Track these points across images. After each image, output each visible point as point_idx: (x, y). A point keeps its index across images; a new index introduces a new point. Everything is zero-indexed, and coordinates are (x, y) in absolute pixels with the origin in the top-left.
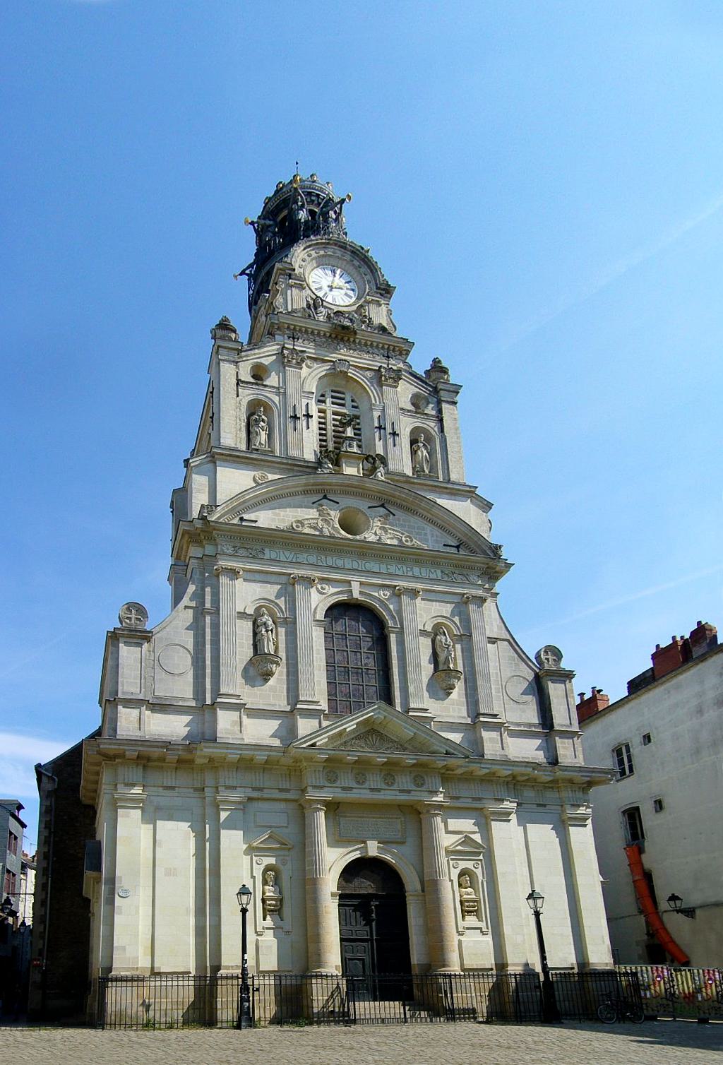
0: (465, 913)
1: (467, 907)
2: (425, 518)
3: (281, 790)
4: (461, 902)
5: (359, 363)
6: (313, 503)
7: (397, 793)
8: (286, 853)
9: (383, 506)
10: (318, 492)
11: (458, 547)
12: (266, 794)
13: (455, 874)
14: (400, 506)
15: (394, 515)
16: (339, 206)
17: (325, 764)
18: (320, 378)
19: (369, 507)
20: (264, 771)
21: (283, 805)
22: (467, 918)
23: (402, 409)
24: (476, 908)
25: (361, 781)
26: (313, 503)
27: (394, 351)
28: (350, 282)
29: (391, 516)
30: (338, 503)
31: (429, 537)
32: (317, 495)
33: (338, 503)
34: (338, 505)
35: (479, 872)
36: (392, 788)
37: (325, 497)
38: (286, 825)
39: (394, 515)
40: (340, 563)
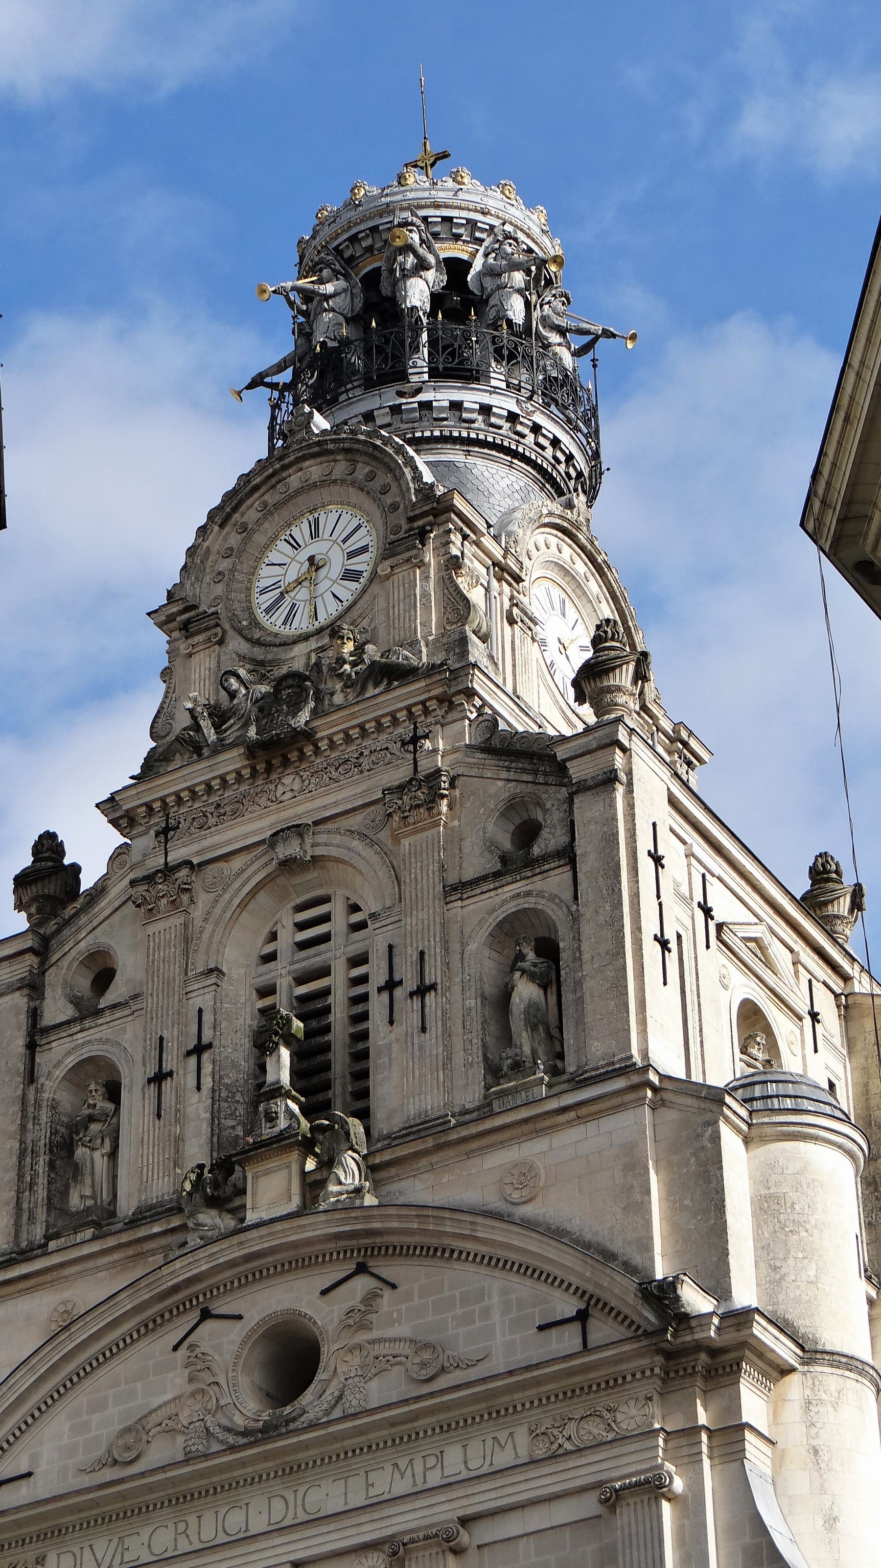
2: (479, 1259)
5: (336, 804)
6: (175, 1348)
9: (362, 1269)
10: (180, 1309)
11: (582, 1317)
14: (404, 1252)
15: (394, 1286)
18: (243, 905)
19: (324, 1293)
23: (454, 888)
26: (175, 1348)
29: (387, 1293)
30: (239, 1317)
31: (496, 1317)
32: (178, 1322)
33: (239, 1317)
34: (237, 1325)
37: (206, 1315)
39: (394, 1286)
40: (235, 1521)
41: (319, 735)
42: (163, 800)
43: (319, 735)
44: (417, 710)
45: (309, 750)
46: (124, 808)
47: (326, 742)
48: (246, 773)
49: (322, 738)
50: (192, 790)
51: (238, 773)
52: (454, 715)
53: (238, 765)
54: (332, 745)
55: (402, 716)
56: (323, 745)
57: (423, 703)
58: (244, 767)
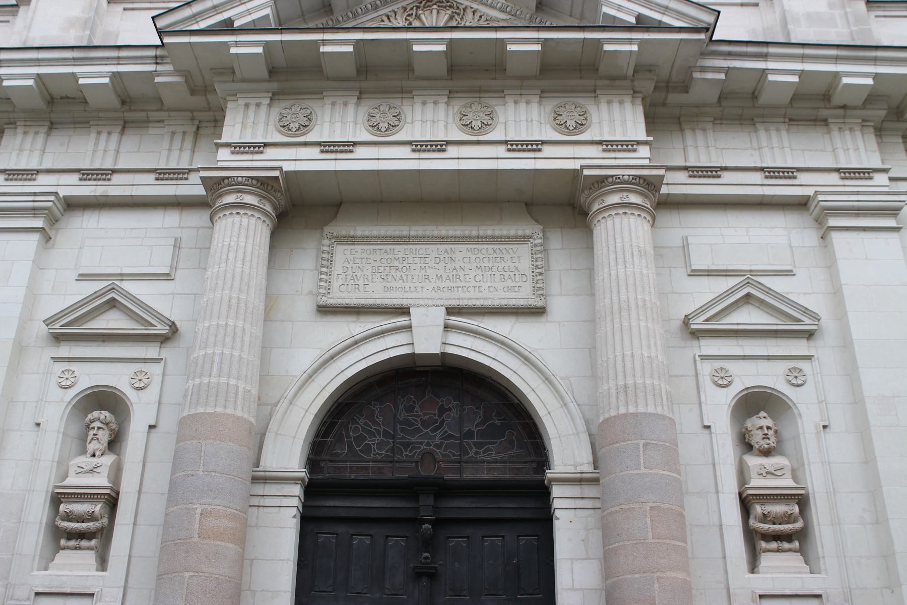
0: (754, 540)
1: (765, 518)
3: (163, 174)
4: (745, 504)
7: (501, 151)
8: (151, 351)
12: (117, 188)
13: (719, 405)
17: (274, 86)
20: (124, 127)
21: (171, 219)
22: (766, 561)
24: (799, 525)
25: (383, 126)
35: (803, 400)
36: (481, 138)
38: (166, 270)
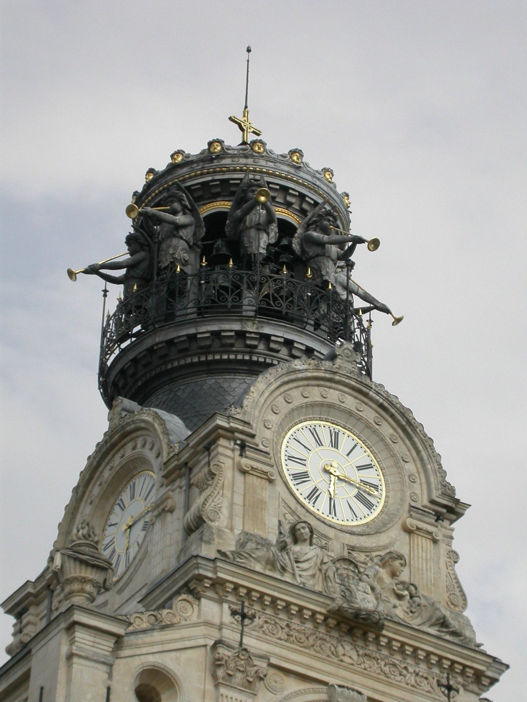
16: (350, 244)
27: (463, 673)
28: (369, 466)
41: (384, 632)
42: (250, 591)
43: (384, 632)
44: (458, 668)
45: (371, 636)
46: (220, 575)
47: (386, 640)
48: (320, 618)
49: (384, 636)
50: (274, 600)
51: (314, 613)
52: (474, 687)
53: (318, 609)
54: (389, 646)
55: (446, 664)
56: (383, 641)
57: (465, 666)
58: (320, 613)
